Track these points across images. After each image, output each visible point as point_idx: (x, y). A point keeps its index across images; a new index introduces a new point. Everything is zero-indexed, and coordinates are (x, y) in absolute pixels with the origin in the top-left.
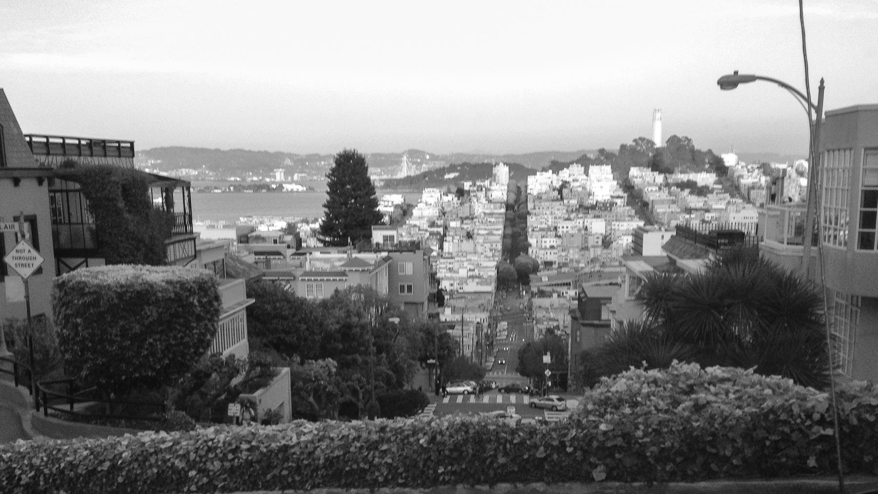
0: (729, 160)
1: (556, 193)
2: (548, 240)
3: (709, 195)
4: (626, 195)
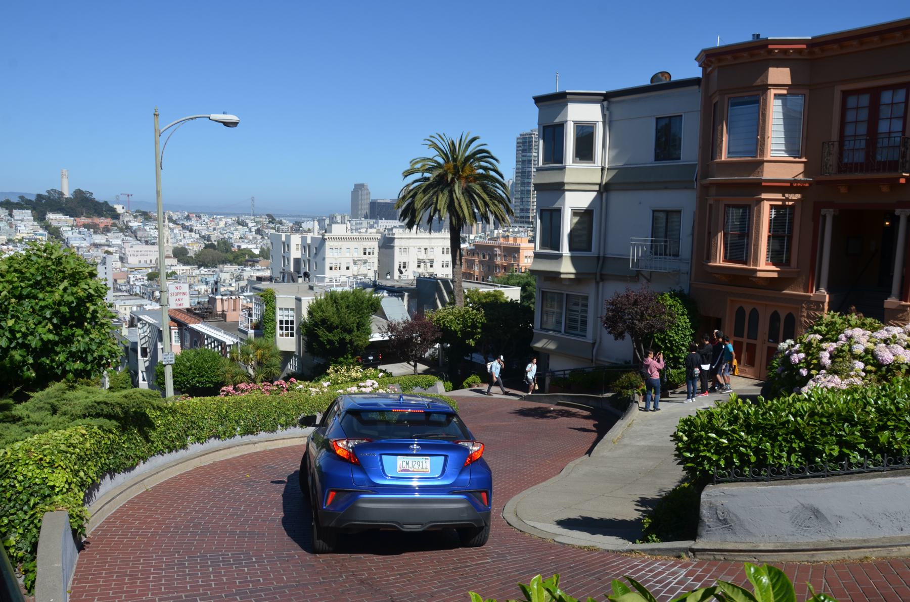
0: (119, 209)
3: (108, 234)
4: (46, 233)
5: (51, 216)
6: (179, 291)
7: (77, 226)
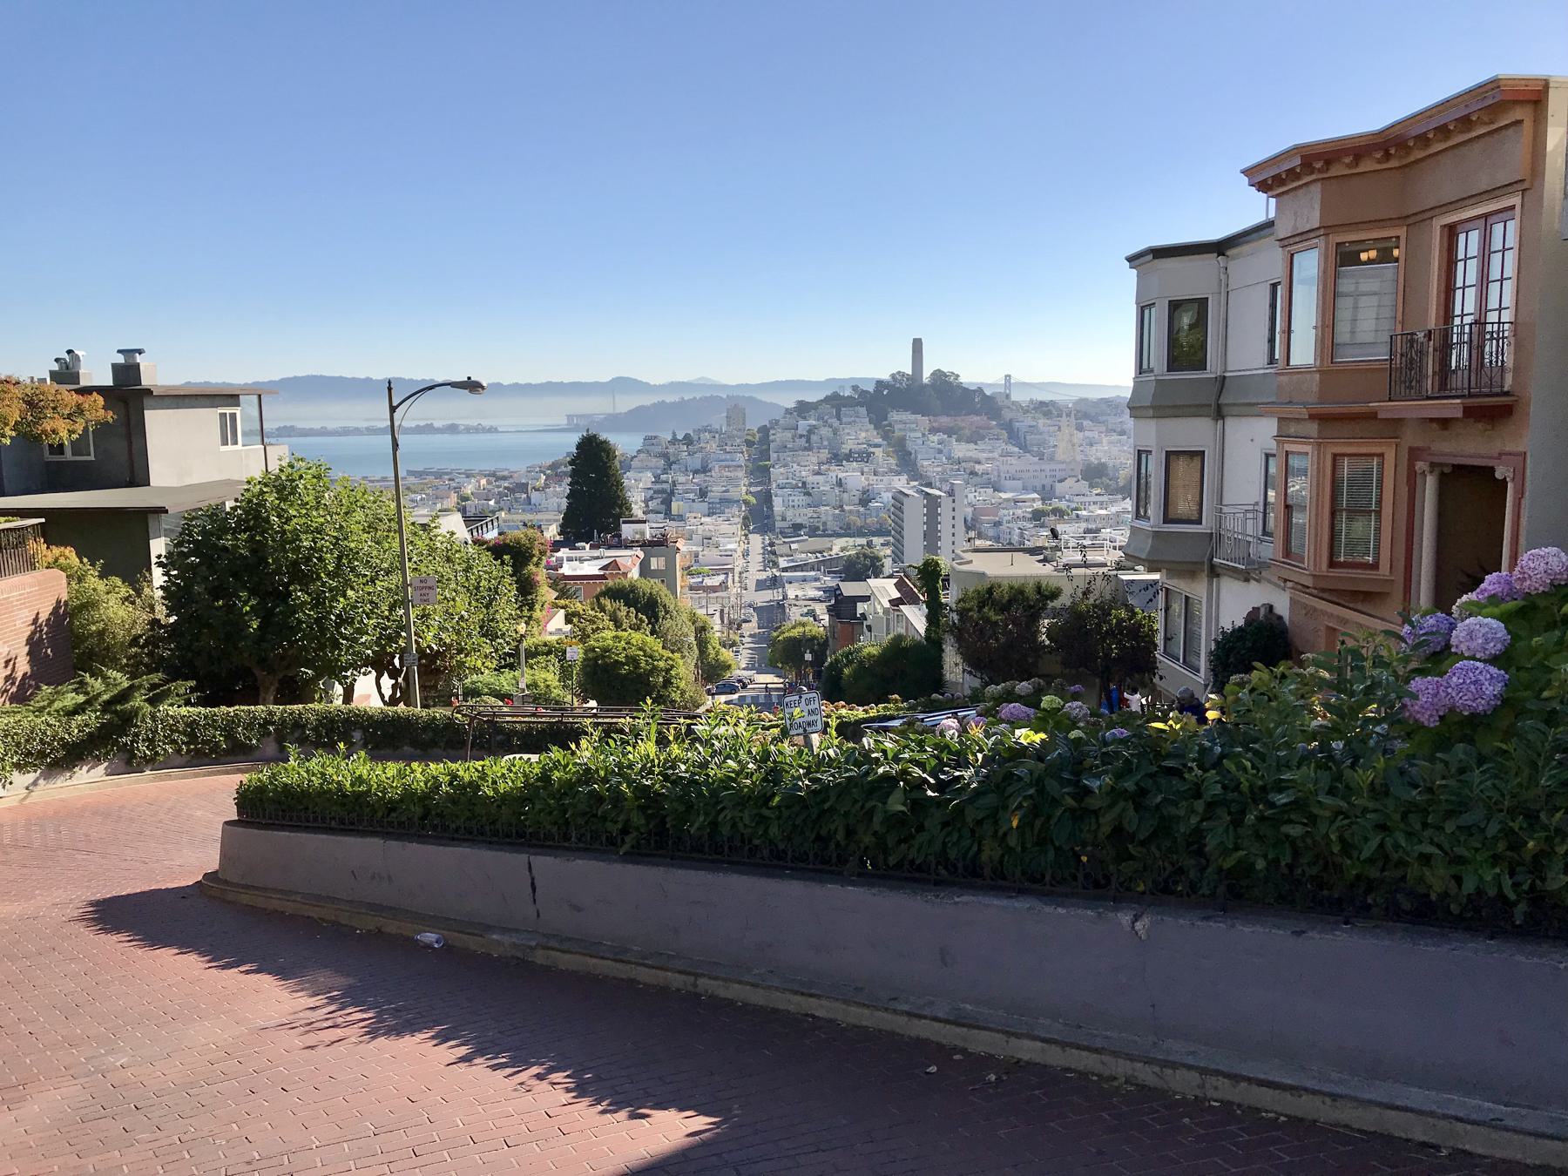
1: (804, 440)
2: (796, 498)
5: (895, 416)
6: (422, 585)
7: (933, 431)
